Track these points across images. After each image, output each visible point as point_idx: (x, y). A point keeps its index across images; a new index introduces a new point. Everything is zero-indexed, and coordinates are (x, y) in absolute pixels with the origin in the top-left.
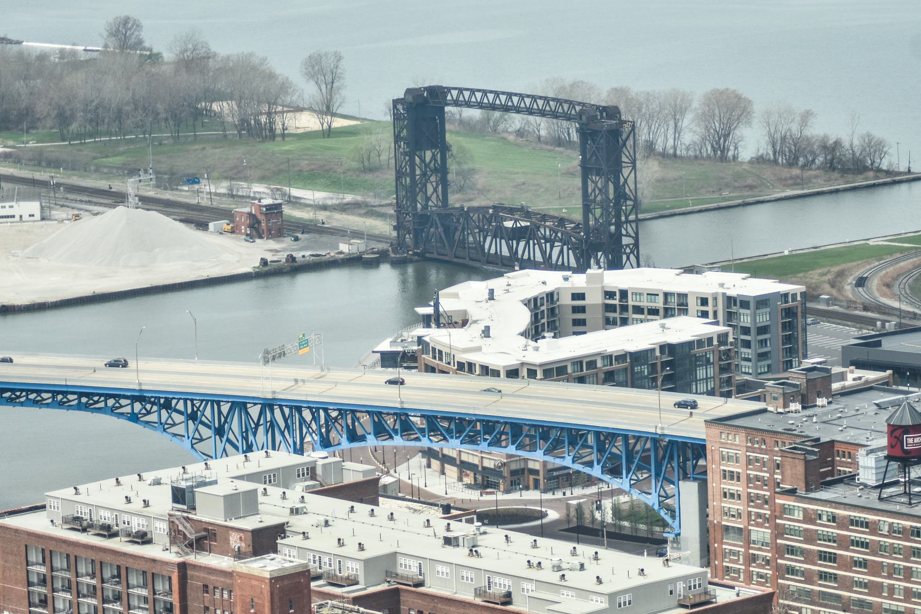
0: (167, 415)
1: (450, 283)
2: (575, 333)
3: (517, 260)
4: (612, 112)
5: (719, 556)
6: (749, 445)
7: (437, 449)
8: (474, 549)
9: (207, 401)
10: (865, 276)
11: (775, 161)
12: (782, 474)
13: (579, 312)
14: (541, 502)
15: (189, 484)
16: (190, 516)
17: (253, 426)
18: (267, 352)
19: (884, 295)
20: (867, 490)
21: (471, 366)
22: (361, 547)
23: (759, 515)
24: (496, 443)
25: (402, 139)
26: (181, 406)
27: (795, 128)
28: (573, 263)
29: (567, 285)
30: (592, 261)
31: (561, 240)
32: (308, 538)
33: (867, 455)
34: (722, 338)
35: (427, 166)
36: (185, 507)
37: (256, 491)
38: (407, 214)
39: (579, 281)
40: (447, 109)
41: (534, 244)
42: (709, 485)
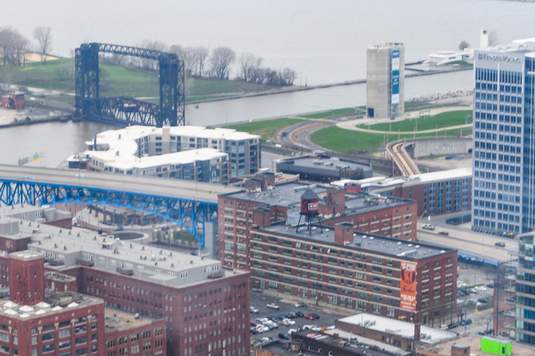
1: (100, 131)
2: (157, 155)
4: (173, 56)
11: (245, 80)
12: (253, 219)
14: (142, 230)
19: (294, 141)
21: (111, 169)
22: (65, 248)
24: (121, 203)
27: (255, 65)
28: (155, 123)
29: (154, 133)
30: (164, 123)
31: (149, 113)
34: (224, 159)
37: (17, 222)
39: (159, 131)
40: (100, 53)
42: (219, 224)
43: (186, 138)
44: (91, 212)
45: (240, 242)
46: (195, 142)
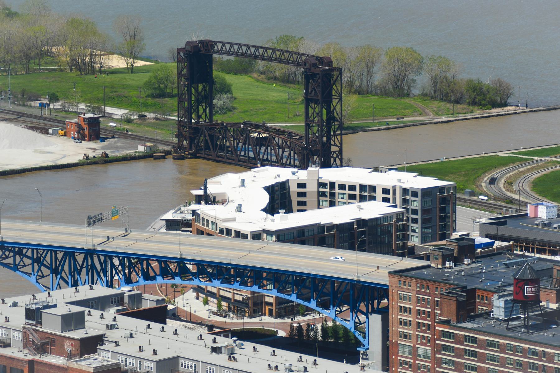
0: (20, 259)
2: (298, 211)
3: (260, 160)
5: (396, 365)
6: (418, 289)
7: (203, 286)
8: (232, 356)
9: (48, 251)
10: (496, 177)
12: (441, 310)
13: (302, 196)
15: (37, 306)
16: (38, 328)
17: (79, 268)
18: (90, 218)
19: (508, 190)
20: (498, 323)
21: (229, 232)
23: (424, 338)
25: (183, 75)
26: (29, 254)
28: (297, 163)
29: (294, 177)
31: (289, 147)
32: (118, 345)
33: (499, 298)
35: (199, 94)
36: (34, 323)
37: (83, 312)
38: (185, 127)
39: (303, 175)
40: (214, 56)
41: (271, 150)
42: (390, 316)
43: (342, 187)
44: (197, 298)
45: (422, 344)
46: (357, 192)
